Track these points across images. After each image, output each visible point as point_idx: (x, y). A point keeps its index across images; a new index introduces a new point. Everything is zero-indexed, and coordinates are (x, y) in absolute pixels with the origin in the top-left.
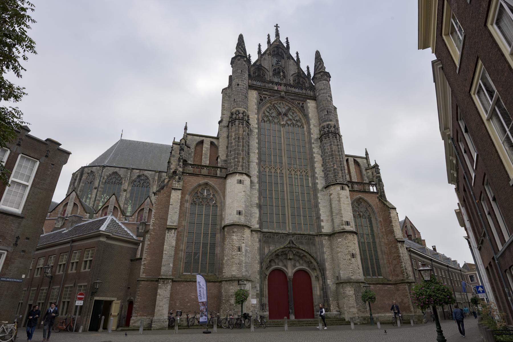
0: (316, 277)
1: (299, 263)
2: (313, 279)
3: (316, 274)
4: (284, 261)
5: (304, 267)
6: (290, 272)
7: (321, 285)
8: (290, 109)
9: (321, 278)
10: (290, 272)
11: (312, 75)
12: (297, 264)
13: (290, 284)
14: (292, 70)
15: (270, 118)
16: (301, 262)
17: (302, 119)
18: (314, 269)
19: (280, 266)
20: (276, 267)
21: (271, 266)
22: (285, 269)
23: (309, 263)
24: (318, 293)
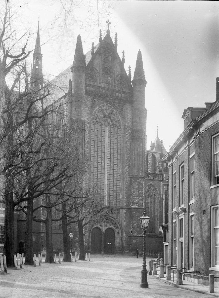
0: (118, 232)
1: (109, 224)
2: (116, 234)
3: (118, 231)
4: (101, 223)
5: (112, 227)
6: (104, 229)
7: (120, 237)
8: (112, 111)
9: (120, 233)
10: (104, 229)
11: (132, 79)
12: (108, 225)
13: (103, 236)
14: (117, 70)
15: (98, 119)
16: (110, 224)
17: (121, 120)
18: (117, 228)
19: (98, 226)
20: (96, 226)
21: (93, 226)
22: (101, 228)
23: (115, 224)
24: (118, 241)
